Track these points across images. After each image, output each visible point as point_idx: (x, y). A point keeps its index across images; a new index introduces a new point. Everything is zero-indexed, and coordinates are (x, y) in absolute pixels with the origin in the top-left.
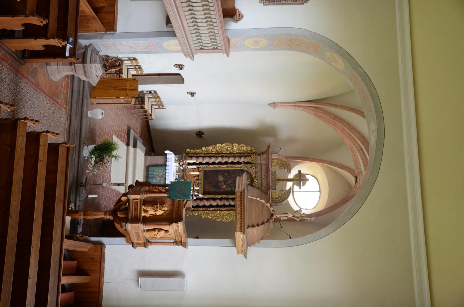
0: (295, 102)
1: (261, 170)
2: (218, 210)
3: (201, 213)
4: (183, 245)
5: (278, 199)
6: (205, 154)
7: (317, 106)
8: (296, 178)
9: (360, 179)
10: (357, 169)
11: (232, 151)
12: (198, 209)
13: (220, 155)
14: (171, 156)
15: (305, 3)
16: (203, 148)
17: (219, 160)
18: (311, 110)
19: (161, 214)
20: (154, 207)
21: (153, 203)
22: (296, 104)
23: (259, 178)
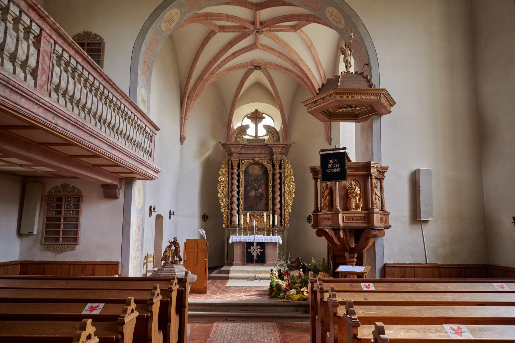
0: (181, 118)
1: (246, 154)
2: (284, 196)
3: (287, 212)
4: (385, 171)
5: (275, 137)
6: (228, 209)
7: (187, 96)
9: (258, 63)
10: (247, 66)
11: (226, 182)
12: (283, 216)
13: (230, 193)
14: (234, 238)
15: (104, 41)
16: (222, 211)
17: (235, 193)
18: (190, 103)
19: (359, 189)
20: (351, 197)
21: (346, 197)
22: (183, 118)
23: (254, 156)
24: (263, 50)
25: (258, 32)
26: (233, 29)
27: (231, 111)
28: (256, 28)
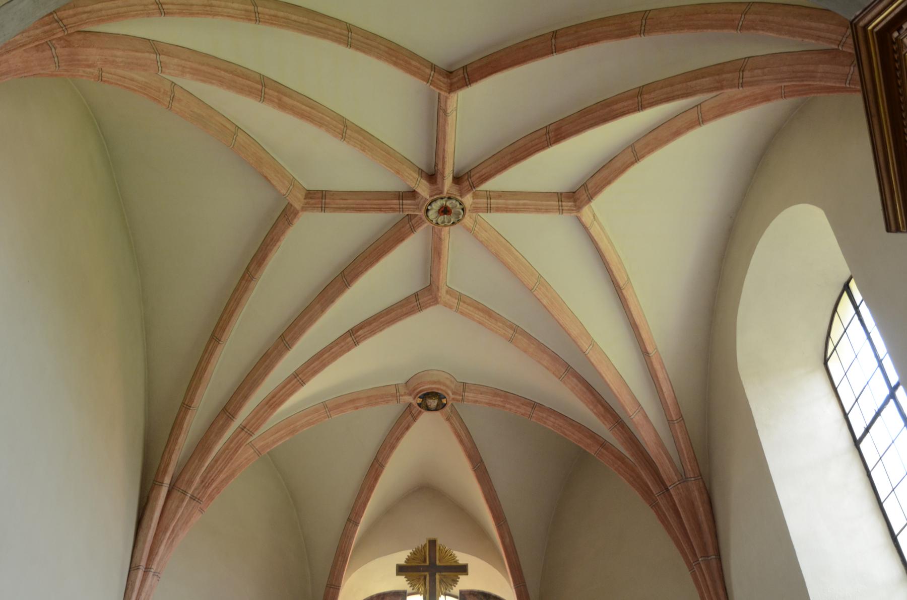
0: (133, 568)
7: (167, 481)
8: (425, 584)
9: (435, 383)
10: (397, 396)
18: (178, 507)
24: (457, 310)
25: (445, 211)
27: (332, 573)
28: (442, 193)
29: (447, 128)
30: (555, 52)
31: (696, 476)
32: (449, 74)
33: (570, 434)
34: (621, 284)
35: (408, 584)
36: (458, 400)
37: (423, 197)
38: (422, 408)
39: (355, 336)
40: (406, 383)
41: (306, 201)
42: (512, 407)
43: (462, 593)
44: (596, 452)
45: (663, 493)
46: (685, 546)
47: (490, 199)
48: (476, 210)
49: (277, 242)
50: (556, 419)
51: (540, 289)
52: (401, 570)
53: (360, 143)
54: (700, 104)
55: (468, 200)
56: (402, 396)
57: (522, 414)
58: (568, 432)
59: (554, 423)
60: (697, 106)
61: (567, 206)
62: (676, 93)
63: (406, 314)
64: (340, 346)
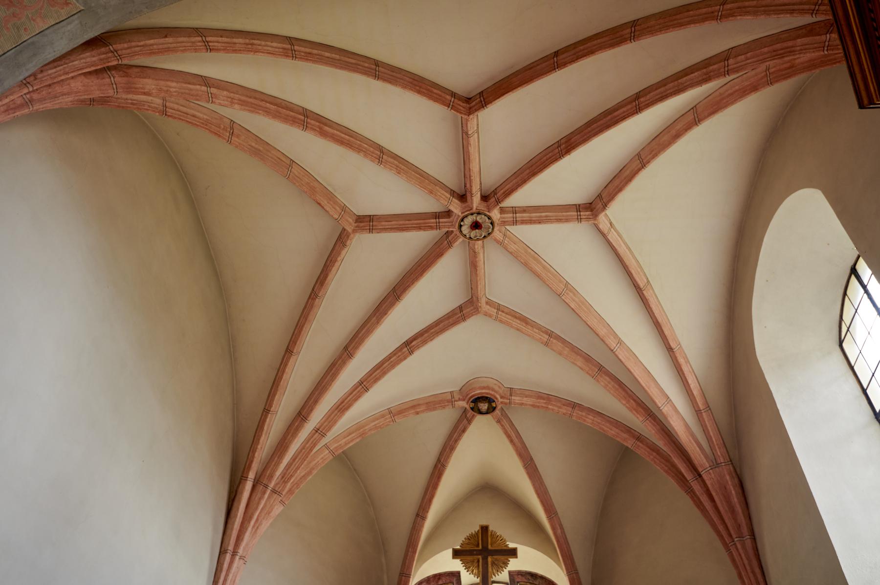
0: (222, 552)
8: (478, 566)
9: (484, 388)
24: (496, 319)
25: (476, 226)
26: (401, 222)
28: (472, 209)
29: (470, 148)
30: (558, 68)
31: (726, 461)
32: (468, 100)
33: (608, 429)
34: (641, 286)
35: (463, 566)
36: (506, 404)
37: (456, 214)
38: (475, 412)
39: (410, 346)
40: (460, 390)
41: (356, 224)
42: (555, 408)
43: (511, 574)
44: (633, 445)
45: (696, 479)
46: (721, 528)
47: (516, 214)
48: (504, 223)
49: (335, 262)
50: (594, 417)
51: (567, 294)
52: (456, 554)
53: (395, 167)
54: (695, 106)
55: (495, 214)
56: (457, 401)
57: (564, 414)
58: (605, 429)
59: (593, 420)
60: (693, 108)
61: (585, 216)
62: (668, 92)
63: (452, 325)
64: (397, 355)
